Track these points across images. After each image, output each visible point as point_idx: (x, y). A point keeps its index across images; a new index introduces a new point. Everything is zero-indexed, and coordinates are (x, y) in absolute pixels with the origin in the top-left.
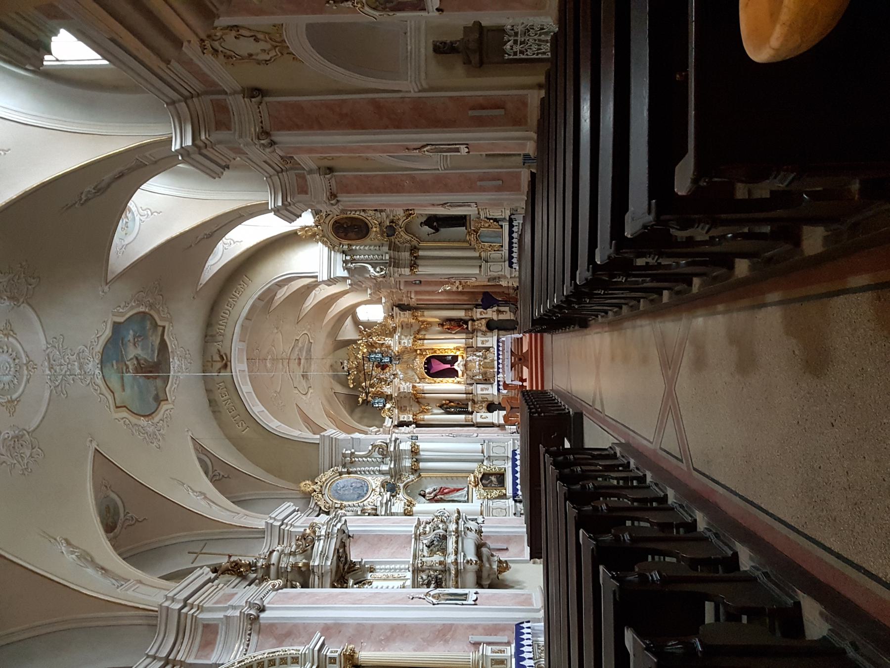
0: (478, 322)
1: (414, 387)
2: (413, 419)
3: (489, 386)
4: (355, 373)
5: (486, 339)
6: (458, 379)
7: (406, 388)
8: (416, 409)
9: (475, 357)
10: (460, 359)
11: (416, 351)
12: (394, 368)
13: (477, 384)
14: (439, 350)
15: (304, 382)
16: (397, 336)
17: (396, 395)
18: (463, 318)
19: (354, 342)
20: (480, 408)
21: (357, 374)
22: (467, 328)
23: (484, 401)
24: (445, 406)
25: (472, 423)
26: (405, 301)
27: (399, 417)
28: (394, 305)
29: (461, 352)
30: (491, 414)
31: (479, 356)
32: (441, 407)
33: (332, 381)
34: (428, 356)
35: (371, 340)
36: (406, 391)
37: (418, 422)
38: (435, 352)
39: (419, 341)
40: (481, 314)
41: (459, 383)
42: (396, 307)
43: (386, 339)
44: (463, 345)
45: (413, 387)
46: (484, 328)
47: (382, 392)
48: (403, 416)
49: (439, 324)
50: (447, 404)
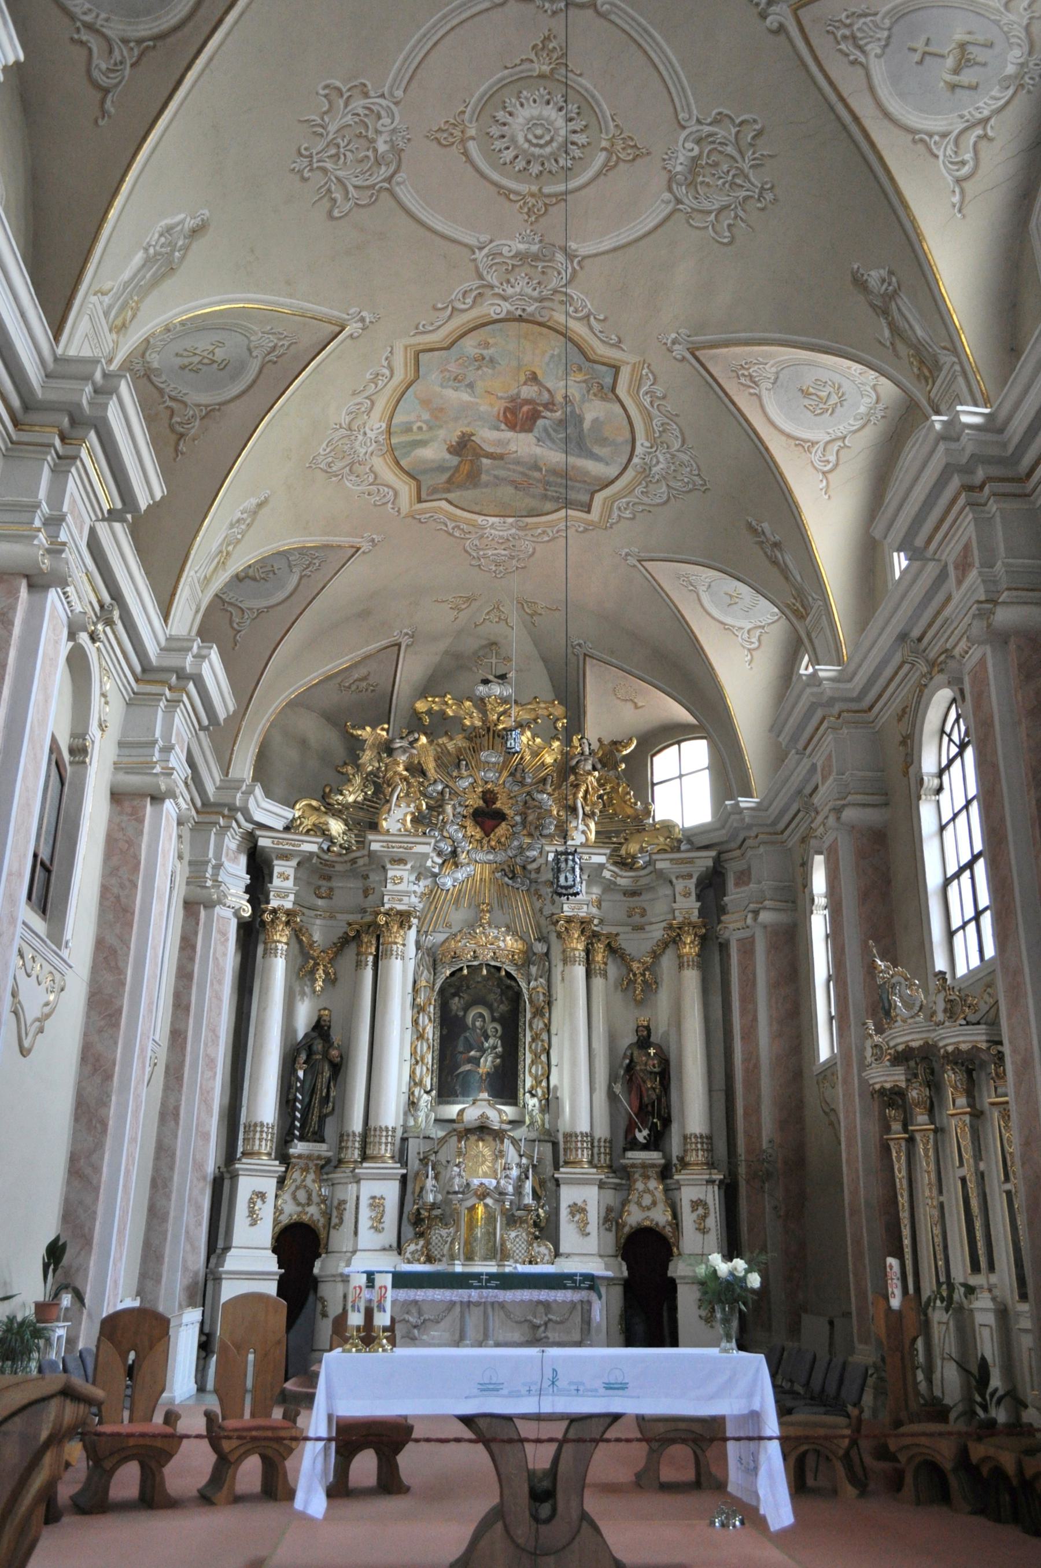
0: (660, 1195)
1: (403, 918)
2: (274, 911)
3: (389, 1236)
4: (467, 722)
5: (593, 1227)
7: (402, 887)
8: (318, 934)
9: (515, 1172)
10: (509, 1111)
11: (542, 939)
12: (480, 856)
13: (404, 1179)
14: (548, 1028)
15: (434, 452)
16: (602, 859)
17: (375, 846)
18: (675, 1127)
19: (576, 723)
20: (302, 1195)
21: (464, 728)
22: (633, 1145)
24: (318, 1046)
25: (239, 1155)
26: (734, 895)
27: (285, 856)
28: (720, 853)
29: (538, 1118)
30: (267, 1239)
31: (519, 1191)
32: (320, 1029)
33: (442, 646)
34: (523, 985)
35: (589, 767)
36: (390, 886)
37: (262, 937)
38: (538, 1012)
39: (581, 946)
40: (696, 1204)
41: (412, 1104)
42: (717, 860)
43: (592, 826)
44: (565, 1124)
45: (400, 913)
46: (634, 1217)
47: (388, 801)
48: (291, 872)
49: (648, 1028)
50: (326, 1054)
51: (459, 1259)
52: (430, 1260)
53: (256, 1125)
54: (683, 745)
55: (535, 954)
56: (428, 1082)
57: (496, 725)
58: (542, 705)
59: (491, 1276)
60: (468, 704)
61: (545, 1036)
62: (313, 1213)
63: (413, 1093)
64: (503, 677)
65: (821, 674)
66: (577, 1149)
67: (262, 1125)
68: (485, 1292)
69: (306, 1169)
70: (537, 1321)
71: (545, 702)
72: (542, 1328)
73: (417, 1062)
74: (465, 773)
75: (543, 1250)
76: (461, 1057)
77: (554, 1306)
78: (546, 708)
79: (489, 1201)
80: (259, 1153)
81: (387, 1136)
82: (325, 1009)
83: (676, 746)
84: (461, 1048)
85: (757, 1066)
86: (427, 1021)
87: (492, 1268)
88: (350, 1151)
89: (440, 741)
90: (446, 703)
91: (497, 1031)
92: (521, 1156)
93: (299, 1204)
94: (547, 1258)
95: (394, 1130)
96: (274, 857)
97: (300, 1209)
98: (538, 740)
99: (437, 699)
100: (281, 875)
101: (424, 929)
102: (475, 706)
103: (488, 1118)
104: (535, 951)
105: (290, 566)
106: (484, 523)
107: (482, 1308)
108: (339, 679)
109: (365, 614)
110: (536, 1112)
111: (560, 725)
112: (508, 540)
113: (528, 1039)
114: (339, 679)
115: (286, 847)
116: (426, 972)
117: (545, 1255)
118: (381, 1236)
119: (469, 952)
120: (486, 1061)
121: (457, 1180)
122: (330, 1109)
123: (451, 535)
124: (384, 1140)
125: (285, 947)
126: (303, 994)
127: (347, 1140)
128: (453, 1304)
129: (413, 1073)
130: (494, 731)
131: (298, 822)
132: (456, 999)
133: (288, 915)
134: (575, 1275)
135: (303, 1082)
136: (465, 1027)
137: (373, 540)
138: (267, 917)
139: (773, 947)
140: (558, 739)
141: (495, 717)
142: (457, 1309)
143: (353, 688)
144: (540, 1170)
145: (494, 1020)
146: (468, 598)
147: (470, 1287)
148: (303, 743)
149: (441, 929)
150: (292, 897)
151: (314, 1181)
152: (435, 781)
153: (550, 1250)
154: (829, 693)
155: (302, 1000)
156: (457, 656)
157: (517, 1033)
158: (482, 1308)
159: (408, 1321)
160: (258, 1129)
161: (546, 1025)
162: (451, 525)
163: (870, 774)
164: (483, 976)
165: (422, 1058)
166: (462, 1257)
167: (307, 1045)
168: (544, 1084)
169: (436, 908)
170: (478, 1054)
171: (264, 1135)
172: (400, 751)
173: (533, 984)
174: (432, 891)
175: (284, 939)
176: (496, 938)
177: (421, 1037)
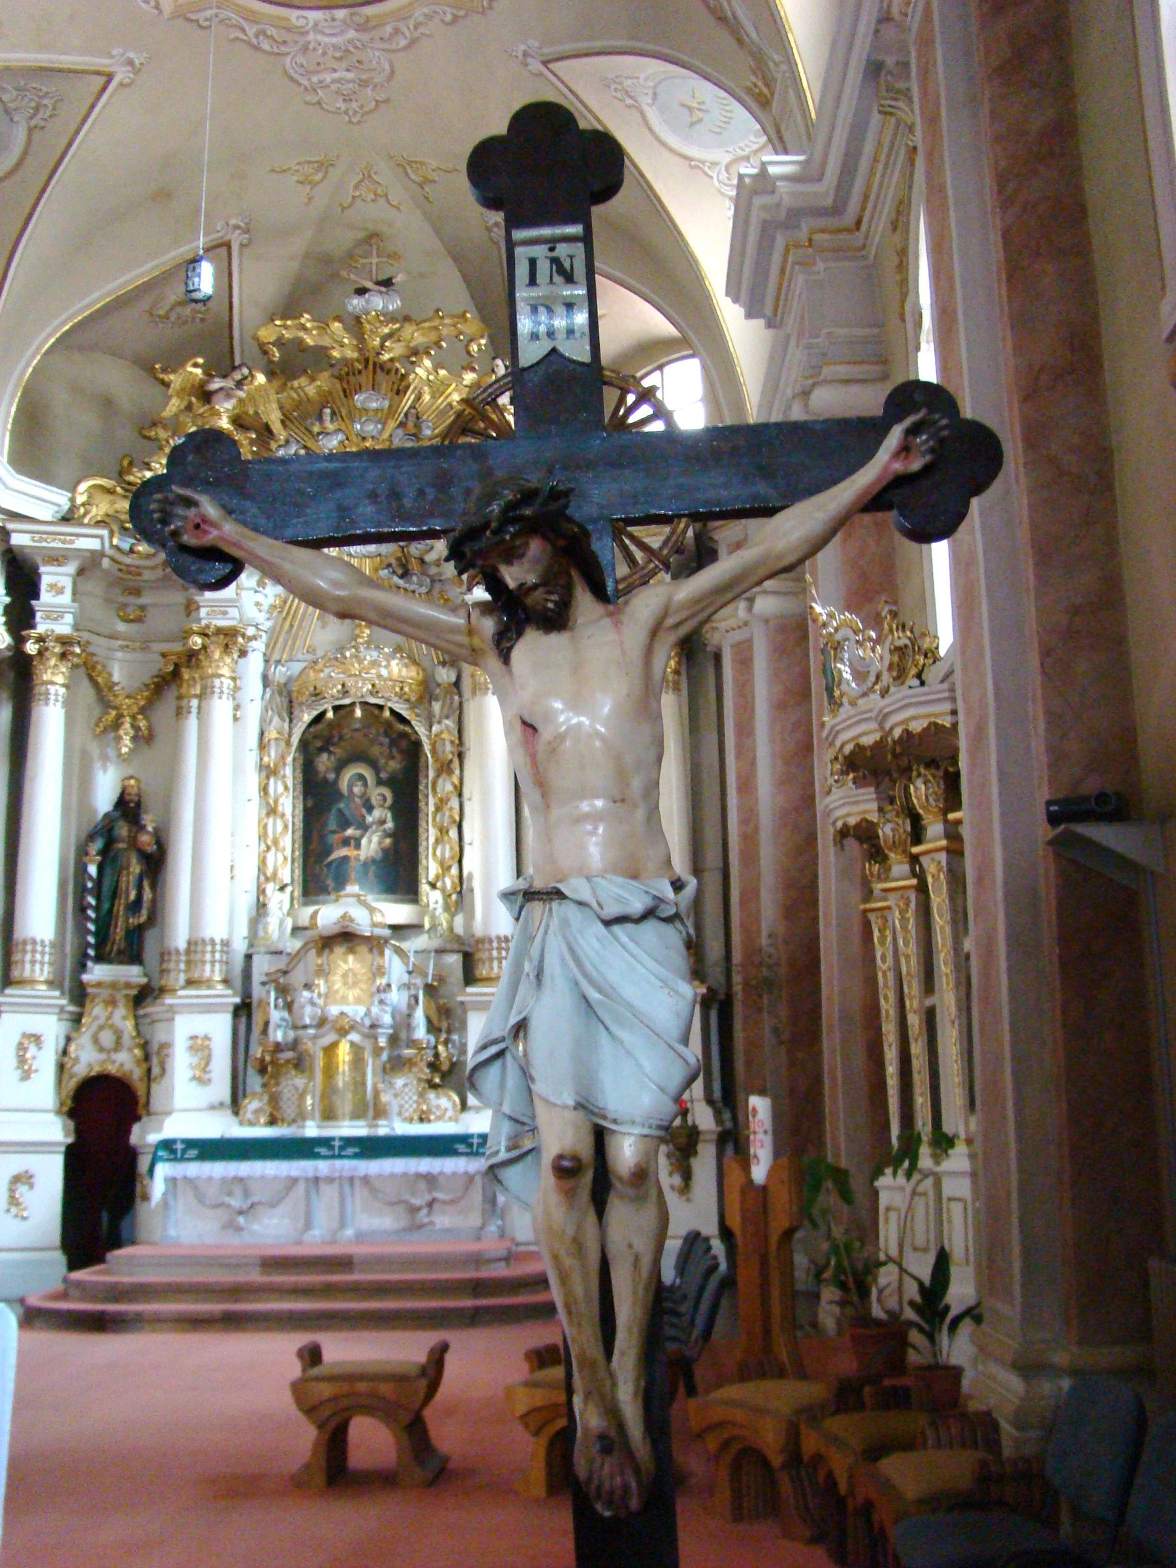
2: (41, 639)
3: (221, 1088)
4: (336, 354)
6: (279, 902)
10: (398, 912)
20: (107, 1038)
23: (147, 1058)
24: (122, 830)
27: (57, 558)
29: (443, 918)
33: (298, 244)
34: (421, 730)
41: (261, 907)
45: (219, 631)
48: (67, 583)
50: (133, 843)
51: (313, 1119)
52: (272, 1122)
53: (25, 942)
54: (666, 369)
55: (439, 685)
56: (285, 875)
57: (379, 354)
58: (447, 321)
59: (349, 1142)
60: (337, 326)
61: (454, 803)
62: (125, 1062)
63: (264, 891)
64: (387, 283)
65: (772, 170)
66: (491, 959)
67: (34, 942)
68: (338, 1163)
69: (112, 1002)
70: (417, 1202)
71: (452, 316)
72: (425, 1211)
73: (268, 848)
74: (330, 427)
75: (444, 1102)
76: (334, 839)
77: (441, 1178)
78: (454, 326)
79: (354, 1037)
80: (33, 982)
81: (213, 952)
82: (131, 777)
83: (658, 373)
84: (332, 824)
85: (756, 829)
86: (281, 789)
87: (358, 1129)
88: (173, 975)
89: (296, 383)
90: (303, 328)
91: (385, 799)
92: (410, 973)
93: (101, 1049)
94: (450, 1113)
95: (226, 944)
96: (39, 561)
97: (103, 1056)
98: (443, 372)
99: (289, 323)
100: (51, 586)
101: (276, 657)
102: (347, 329)
103: (352, 920)
104: (439, 680)
105: (7, 111)
106: (302, 22)
107: (336, 1185)
108: (145, 304)
109: (163, 196)
110: (439, 911)
111: (474, 348)
112: (347, 51)
113: (431, 808)
114: (145, 304)
115: (53, 545)
116: (276, 719)
117: (446, 1110)
118: (208, 1089)
119: (334, 686)
120: (370, 842)
121: (308, 1010)
122: (143, 919)
123: (257, 48)
124: (208, 957)
125: (62, 691)
126: (104, 758)
127: (170, 960)
128: (294, 1181)
129: (263, 862)
130: (375, 364)
131: (82, 510)
132: (325, 756)
133: (64, 644)
134: (472, 1136)
135: (99, 882)
136: (338, 796)
137: (130, 63)
138: (31, 648)
139: (779, 651)
140: (473, 370)
141: (377, 342)
142: (301, 1188)
143: (173, 317)
144: (443, 991)
145: (380, 782)
146: (321, 164)
147: (317, 1156)
148: (107, 404)
149: (300, 656)
150: (69, 618)
151: (125, 1018)
152: (287, 442)
153: (454, 1103)
154: (787, 201)
155: (105, 770)
156: (326, 260)
157: (415, 800)
158: (336, 1185)
159: (229, 1206)
160: (29, 948)
161: (455, 787)
162: (251, 30)
163: (861, 332)
164: (360, 720)
165: (276, 842)
166: (317, 1115)
167: (105, 831)
168: (454, 871)
169: (291, 626)
170: (358, 833)
171: (38, 957)
172: (221, 395)
173: (435, 728)
174: (285, 602)
175: (60, 679)
176: (375, 664)
177: (272, 811)
